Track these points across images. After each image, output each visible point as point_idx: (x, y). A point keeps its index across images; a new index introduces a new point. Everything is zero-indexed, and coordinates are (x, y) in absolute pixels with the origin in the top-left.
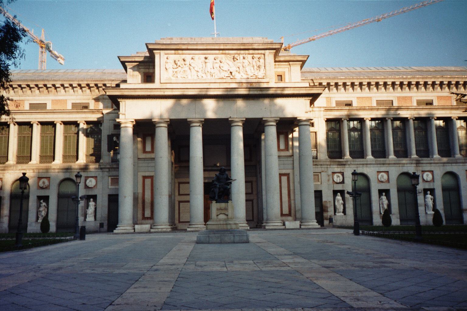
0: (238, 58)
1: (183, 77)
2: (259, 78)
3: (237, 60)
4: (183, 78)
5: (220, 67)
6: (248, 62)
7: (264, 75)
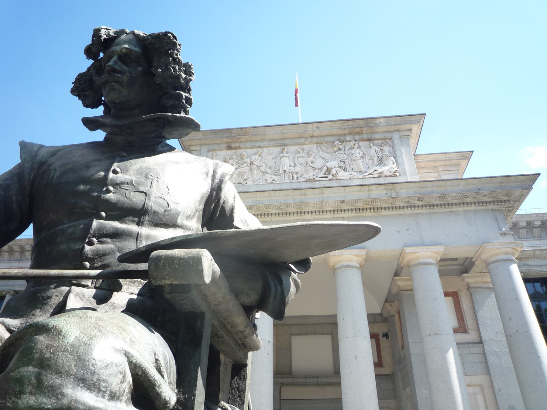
1: (236, 183)
3: (340, 150)
4: (238, 185)
5: (307, 163)
6: (361, 153)
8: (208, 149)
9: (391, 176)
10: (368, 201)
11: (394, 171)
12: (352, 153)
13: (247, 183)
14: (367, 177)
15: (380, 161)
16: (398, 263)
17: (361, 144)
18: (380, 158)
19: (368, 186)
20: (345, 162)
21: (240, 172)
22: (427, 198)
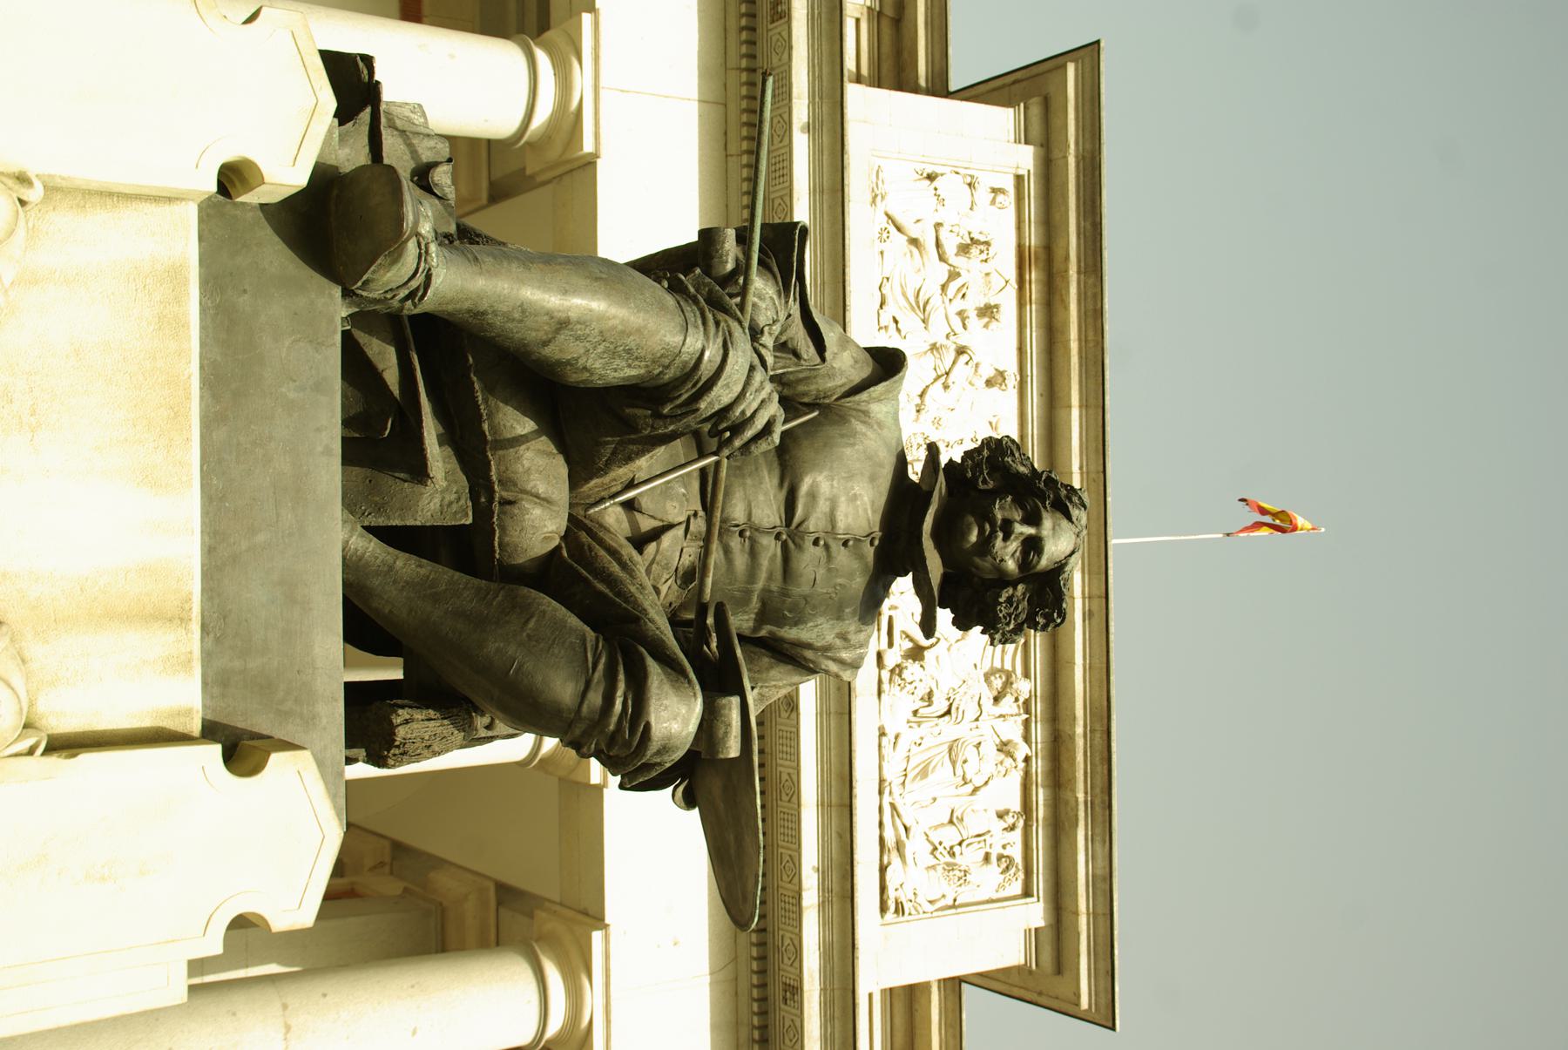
0: (1008, 704)
2: (883, 870)
3: (996, 700)
7: (907, 906)
8: (1029, 171)
9: (883, 889)
10: (789, 801)
11: (901, 903)
12: (980, 743)
13: (883, 331)
14: (887, 799)
15: (945, 848)
16: (549, 901)
17: (1016, 778)
18: (957, 849)
19: (849, 804)
20: (947, 718)
21: (926, 303)
22: (794, 1018)
